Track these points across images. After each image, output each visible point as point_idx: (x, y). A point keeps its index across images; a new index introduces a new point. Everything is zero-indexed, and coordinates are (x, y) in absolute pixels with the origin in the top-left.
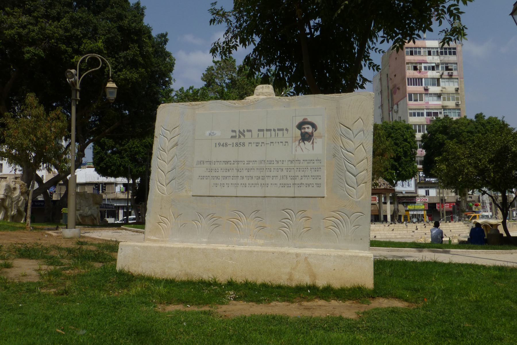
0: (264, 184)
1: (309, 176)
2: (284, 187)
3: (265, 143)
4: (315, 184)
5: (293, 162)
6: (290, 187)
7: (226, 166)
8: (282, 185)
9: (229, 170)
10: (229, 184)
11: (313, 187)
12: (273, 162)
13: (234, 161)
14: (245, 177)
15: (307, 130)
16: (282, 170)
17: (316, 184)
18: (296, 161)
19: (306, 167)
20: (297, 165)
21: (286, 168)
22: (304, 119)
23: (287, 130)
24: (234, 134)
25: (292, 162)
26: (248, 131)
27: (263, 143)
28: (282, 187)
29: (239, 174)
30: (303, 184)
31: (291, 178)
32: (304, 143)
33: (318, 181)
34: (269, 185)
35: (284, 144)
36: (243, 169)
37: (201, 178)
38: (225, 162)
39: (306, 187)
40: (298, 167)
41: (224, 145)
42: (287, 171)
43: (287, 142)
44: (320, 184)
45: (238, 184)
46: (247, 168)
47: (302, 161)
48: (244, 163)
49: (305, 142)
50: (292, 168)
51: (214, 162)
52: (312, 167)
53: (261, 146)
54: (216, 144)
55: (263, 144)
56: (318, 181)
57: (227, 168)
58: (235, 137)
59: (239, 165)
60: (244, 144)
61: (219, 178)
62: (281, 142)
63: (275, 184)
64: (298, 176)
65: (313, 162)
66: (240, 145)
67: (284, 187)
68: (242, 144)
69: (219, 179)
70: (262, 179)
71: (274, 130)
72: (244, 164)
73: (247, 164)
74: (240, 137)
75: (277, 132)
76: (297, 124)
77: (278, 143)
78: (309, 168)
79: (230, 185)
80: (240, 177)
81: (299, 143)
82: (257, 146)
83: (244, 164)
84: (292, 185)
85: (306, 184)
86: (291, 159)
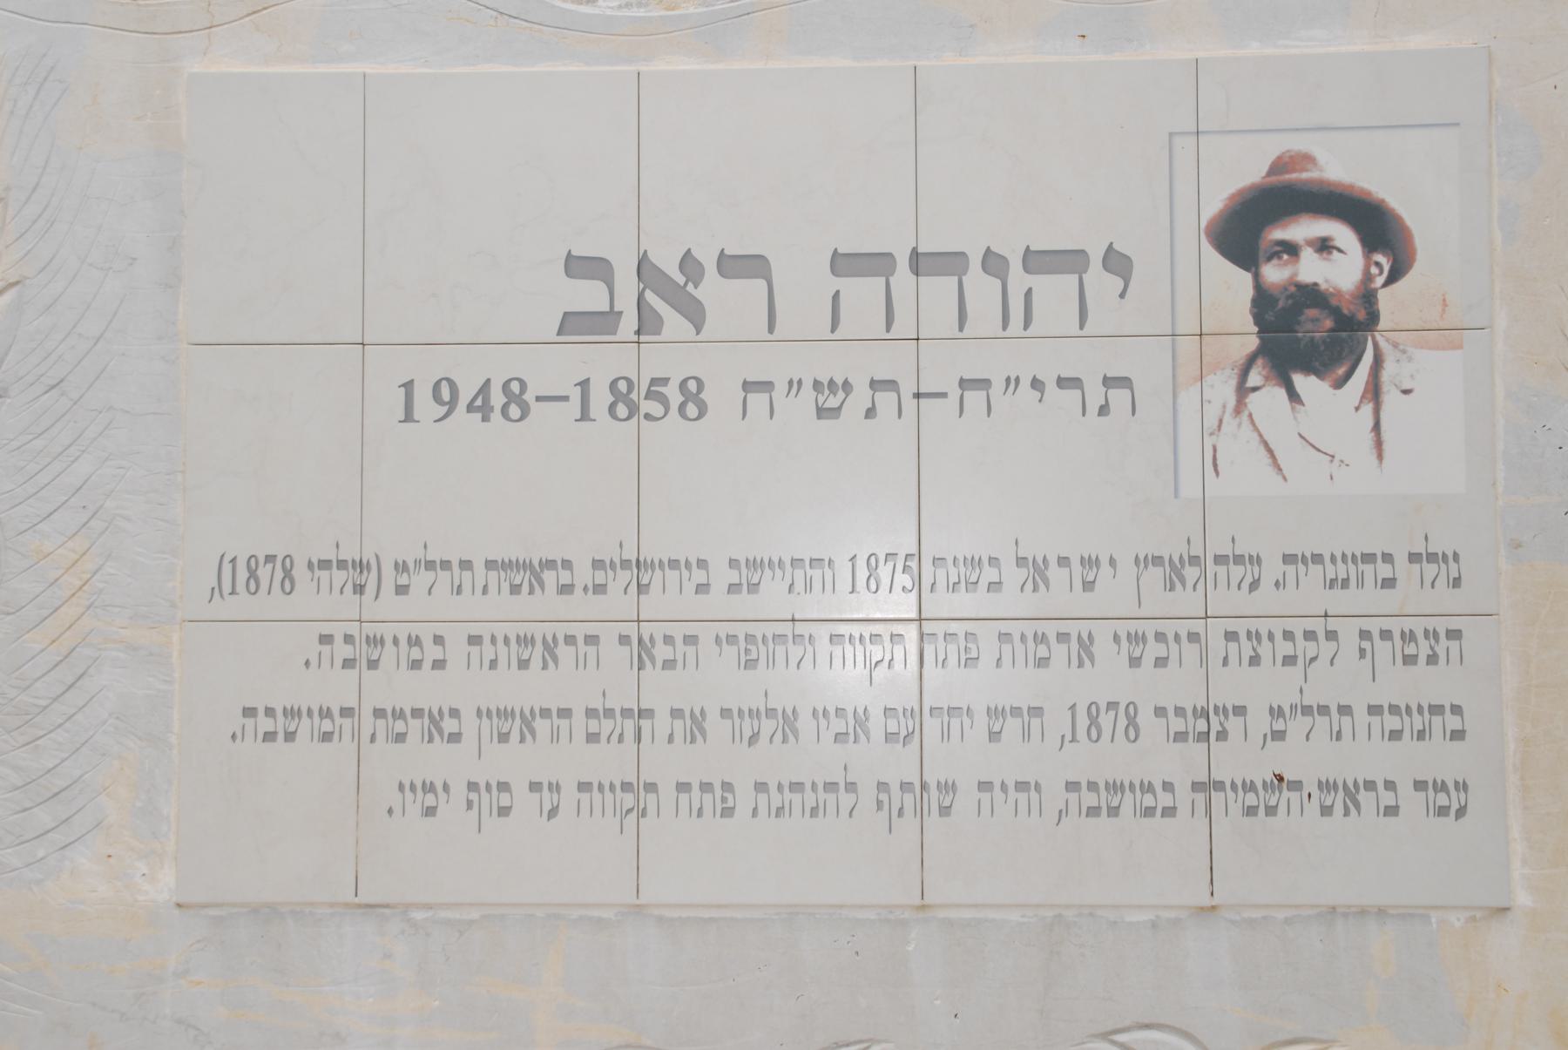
0: (905, 787)
1: (1345, 710)
2: (1114, 811)
3: (907, 389)
4: (1406, 788)
5: (1191, 573)
6: (1169, 812)
7: (524, 605)
8: (1090, 799)
9: (550, 648)
10: (555, 788)
11: (1392, 811)
12: (990, 574)
13: (597, 564)
14: (713, 722)
15: (1311, 269)
16: (1086, 646)
17: (1420, 785)
18: (1220, 560)
19: (1317, 625)
20: (1227, 600)
21: (1123, 628)
22: (1278, 166)
23: (1117, 263)
24: (590, 296)
25: (1175, 575)
26: (734, 266)
27: (891, 385)
28: (1093, 811)
29: (660, 690)
30: (1296, 786)
31: (1178, 725)
32: (1293, 396)
33: (1439, 759)
34: (966, 800)
35: (1095, 398)
36: (691, 640)
37: (266, 724)
38: (507, 566)
39: (1326, 811)
40: (1241, 627)
41: (498, 399)
42: (1135, 662)
43: (1124, 382)
44: (1462, 786)
45: (651, 787)
46: (740, 630)
47: (1272, 569)
48: (699, 576)
49: (1301, 381)
50: (1183, 628)
51: (401, 567)
52: (1374, 626)
53: (870, 413)
54: (408, 386)
55: (886, 400)
56: (1439, 759)
57: (538, 631)
58: (604, 322)
59: (652, 605)
60: (693, 396)
61: (449, 725)
62: (1062, 382)
63: (1022, 786)
64: (1240, 711)
65: (1385, 571)
66: (655, 408)
67: (1114, 811)
68: (676, 399)
69: (455, 738)
70: (890, 737)
71: (993, 263)
72: (702, 588)
73: (733, 588)
74: (647, 323)
75: (1018, 280)
76: (1214, 205)
77: (1036, 384)
78: (1348, 632)
79: (569, 794)
80: (662, 722)
81: (1243, 391)
82: (822, 412)
83: (702, 588)
84: (1184, 796)
85: (1327, 786)
86: (1173, 548)
